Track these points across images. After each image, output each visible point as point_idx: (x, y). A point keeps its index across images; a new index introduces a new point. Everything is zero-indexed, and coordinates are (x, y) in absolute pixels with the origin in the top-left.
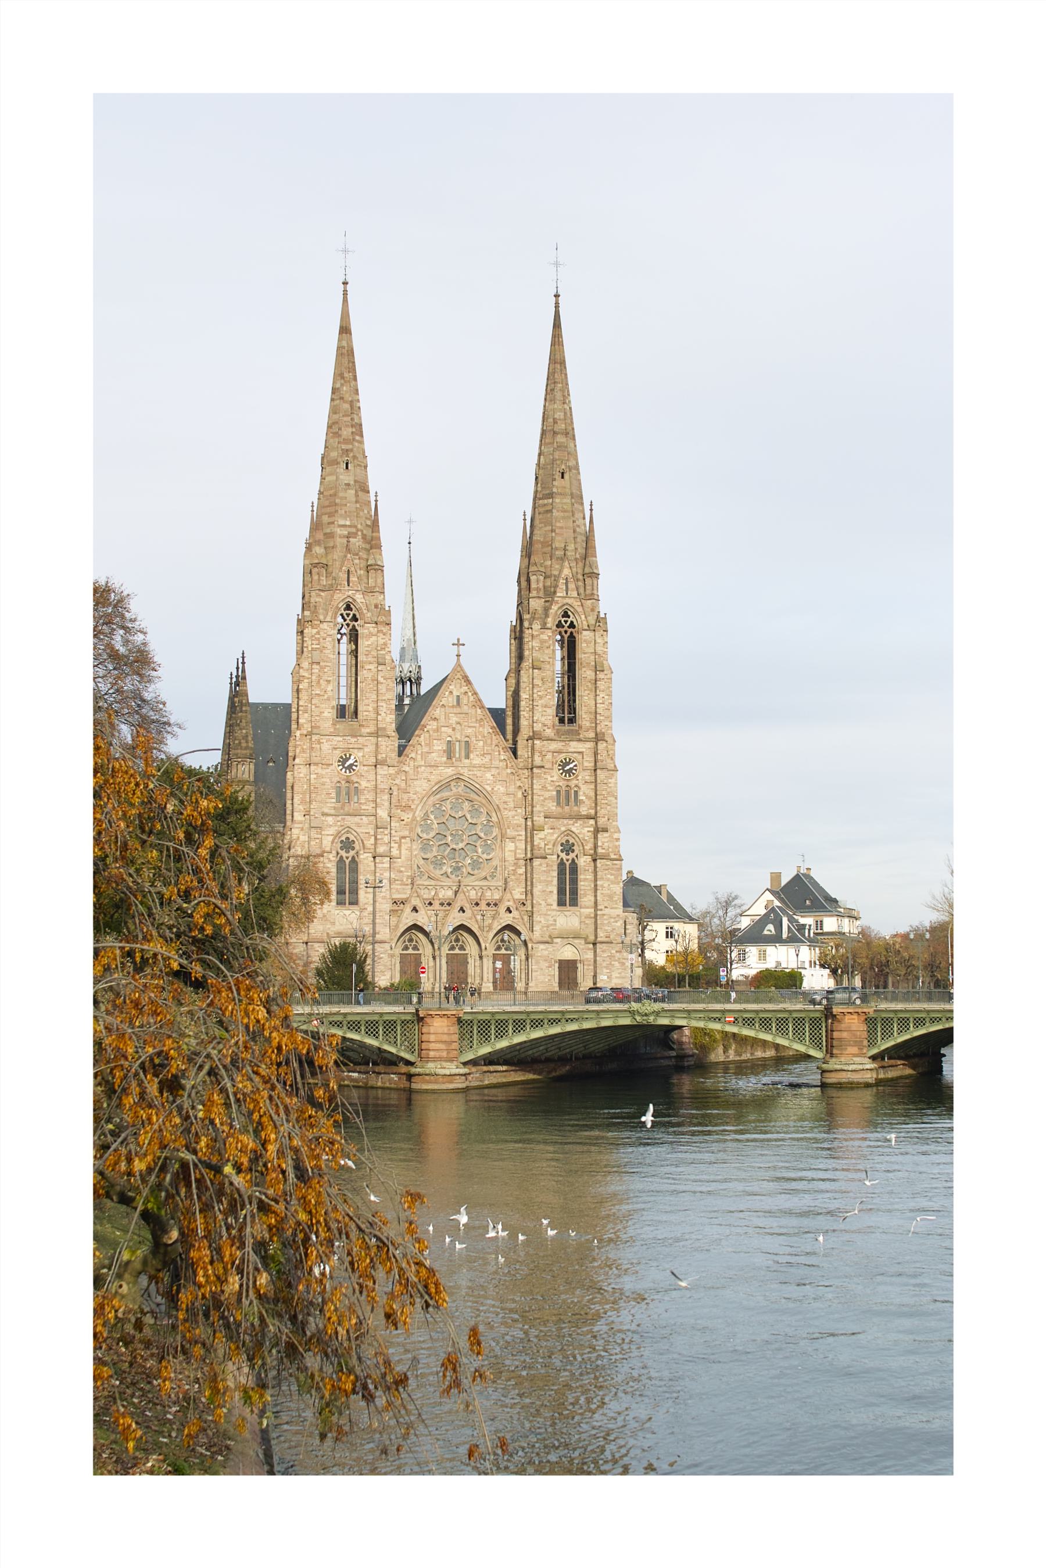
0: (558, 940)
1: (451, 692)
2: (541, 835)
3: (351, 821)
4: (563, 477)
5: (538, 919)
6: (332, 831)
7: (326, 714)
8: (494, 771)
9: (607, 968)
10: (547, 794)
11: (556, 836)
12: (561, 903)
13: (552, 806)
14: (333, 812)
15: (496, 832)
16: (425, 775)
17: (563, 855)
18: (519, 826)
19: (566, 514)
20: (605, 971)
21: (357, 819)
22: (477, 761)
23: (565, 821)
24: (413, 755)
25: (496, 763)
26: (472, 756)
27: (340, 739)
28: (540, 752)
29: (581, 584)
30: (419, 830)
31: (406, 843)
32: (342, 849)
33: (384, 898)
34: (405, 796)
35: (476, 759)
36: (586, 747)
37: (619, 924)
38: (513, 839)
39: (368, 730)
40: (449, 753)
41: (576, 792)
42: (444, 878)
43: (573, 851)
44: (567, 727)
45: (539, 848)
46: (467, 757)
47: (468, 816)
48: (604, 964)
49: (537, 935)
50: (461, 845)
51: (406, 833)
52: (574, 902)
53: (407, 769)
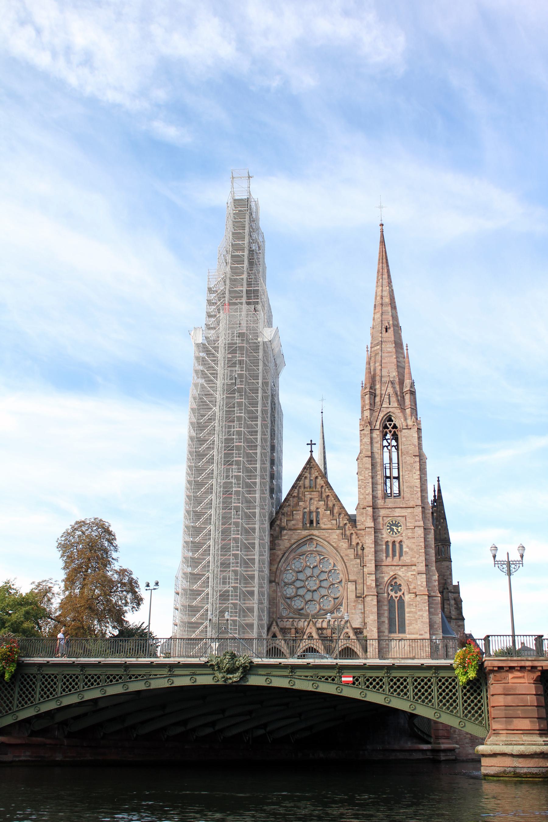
4: (386, 331)
17: (393, 594)
19: (390, 354)
23: (393, 568)
43: (400, 590)
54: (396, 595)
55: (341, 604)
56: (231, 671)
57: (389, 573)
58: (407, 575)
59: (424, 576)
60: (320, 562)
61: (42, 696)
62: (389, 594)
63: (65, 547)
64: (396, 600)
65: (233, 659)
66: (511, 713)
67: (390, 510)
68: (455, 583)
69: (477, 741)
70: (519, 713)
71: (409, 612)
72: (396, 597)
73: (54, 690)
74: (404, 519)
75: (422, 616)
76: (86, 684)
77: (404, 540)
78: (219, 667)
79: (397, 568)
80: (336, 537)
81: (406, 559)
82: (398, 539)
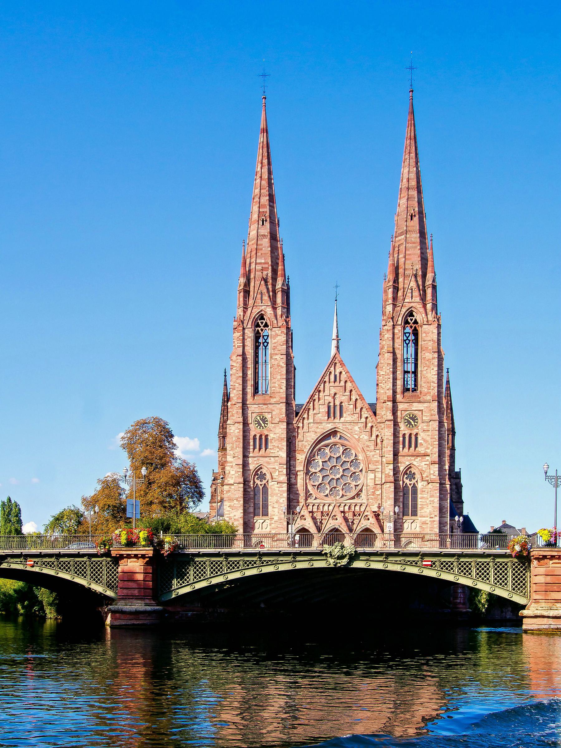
16: (313, 429)
18: (377, 462)
23: (409, 458)
27: (256, 406)
35: (347, 417)
38: (373, 471)
39: (275, 400)
41: (416, 439)
42: (326, 498)
43: (414, 478)
46: (341, 416)
54: (411, 483)
55: (361, 490)
56: (341, 557)
57: (405, 463)
58: (421, 464)
59: (437, 466)
60: (343, 453)
61: (195, 577)
62: (404, 482)
64: (410, 487)
65: (342, 549)
66: (549, 588)
67: (408, 404)
68: (457, 470)
69: (523, 607)
70: (555, 588)
71: (422, 498)
72: (410, 484)
73: (205, 573)
75: (433, 501)
76: (229, 568)
77: (420, 433)
78: (331, 555)
79: (413, 458)
80: (358, 430)
81: (420, 449)
82: (414, 432)
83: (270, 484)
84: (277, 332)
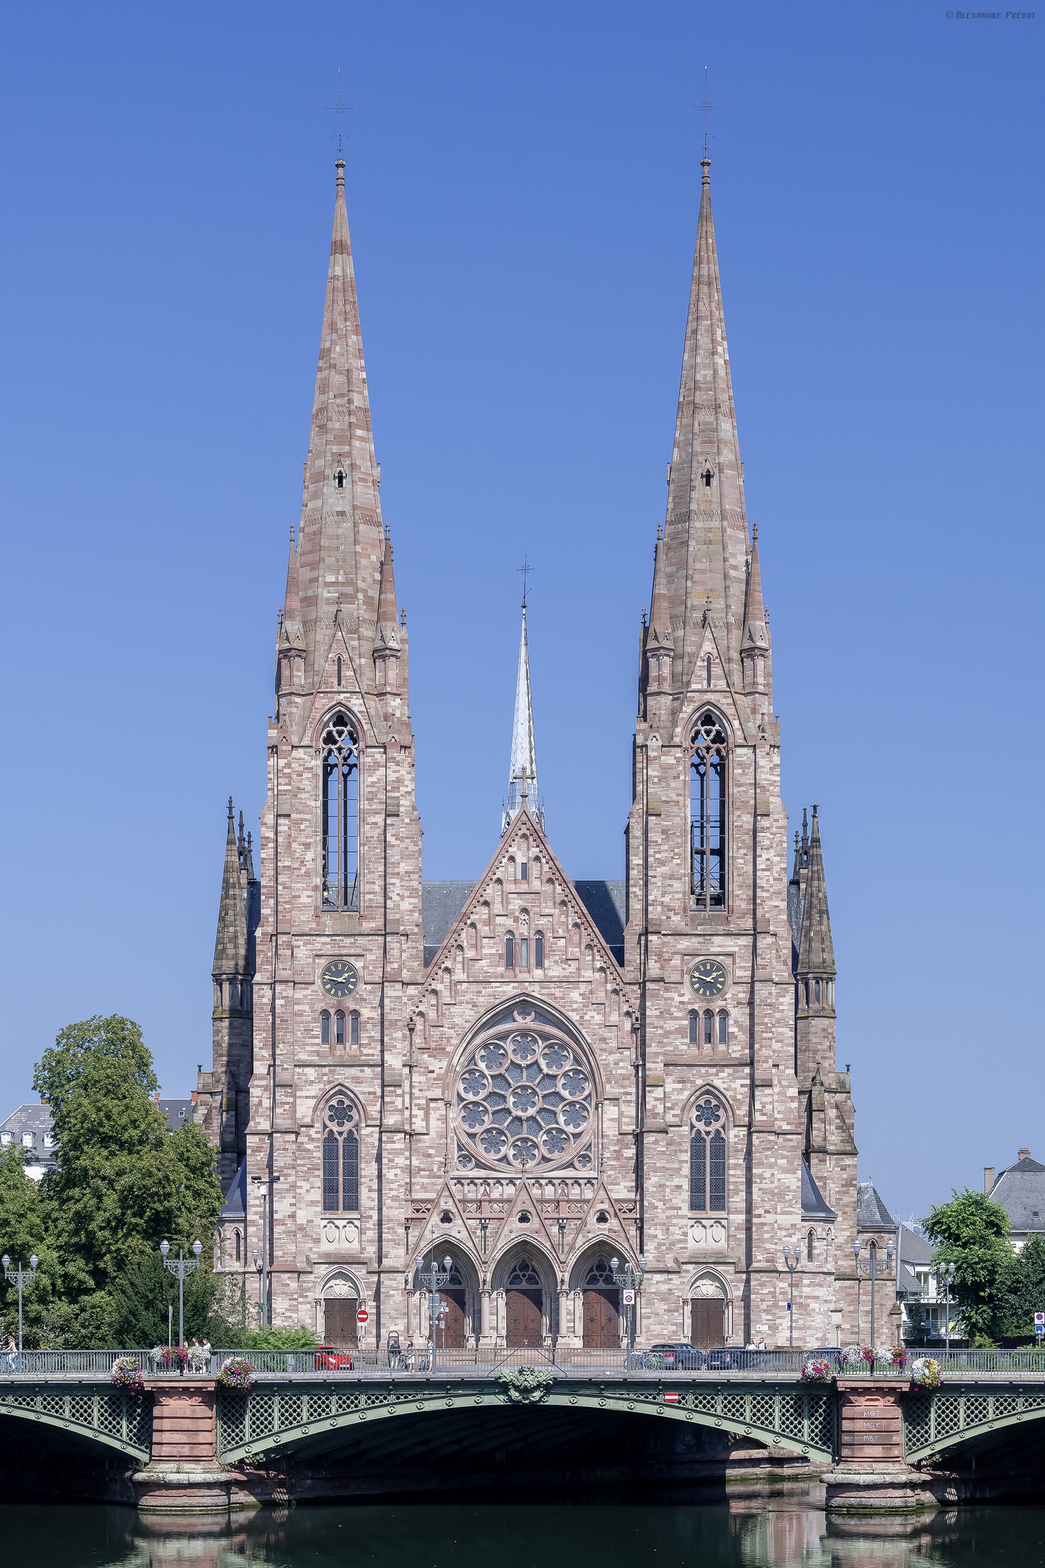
0: (690, 1267)
1: (512, 859)
2: (658, 1092)
3: (344, 1075)
5: (652, 1231)
6: (315, 1090)
7: (304, 899)
8: (583, 988)
9: (767, 1311)
10: (671, 1025)
11: (686, 1093)
12: (696, 1205)
13: (682, 1045)
14: (315, 1059)
15: (588, 1087)
16: (468, 997)
17: (700, 1126)
18: (625, 1077)
20: (764, 1316)
21: (354, 1071)
22: (555, 971)
23: (703, 1070)
24: (448, 964)
25: (588, 974)
26: (547, 963)
27: (327, 939)
28: (659, 955)
29: (735, 667)
30: (461, 1087)
31: (438, 1110)
32: (331, 1118)
33: (395, 1199)
34: (435, 1032)
36: (738, 945)
37: (794, 1239)
38: (615, 1100)
39: (373, 925)
40: (510, 959)
42: (503, 1165)
44: (709, 911)
45: (655, 1115)
46: (540, 964)
47: (543, 1063)
48: (764, 1306)
49: (650, 1257)
50: (531, 1111)
51: (437, 1093)
52: (719, 1202)
53: (439, 987)
54: (708, 1129)
57: (693, 1082)
58: (733, 1086)
62: (692, 1127)
63: (53, 1080)
67: (701, 939)
70: (870, 1438)
72: (708, 1133)
73: (299, 1415)
74: (728, 961)
76: (340, 1407)
79: (713, 1070)
80: (580, 999)
83: (363, 1132)
84: (378, 756)
